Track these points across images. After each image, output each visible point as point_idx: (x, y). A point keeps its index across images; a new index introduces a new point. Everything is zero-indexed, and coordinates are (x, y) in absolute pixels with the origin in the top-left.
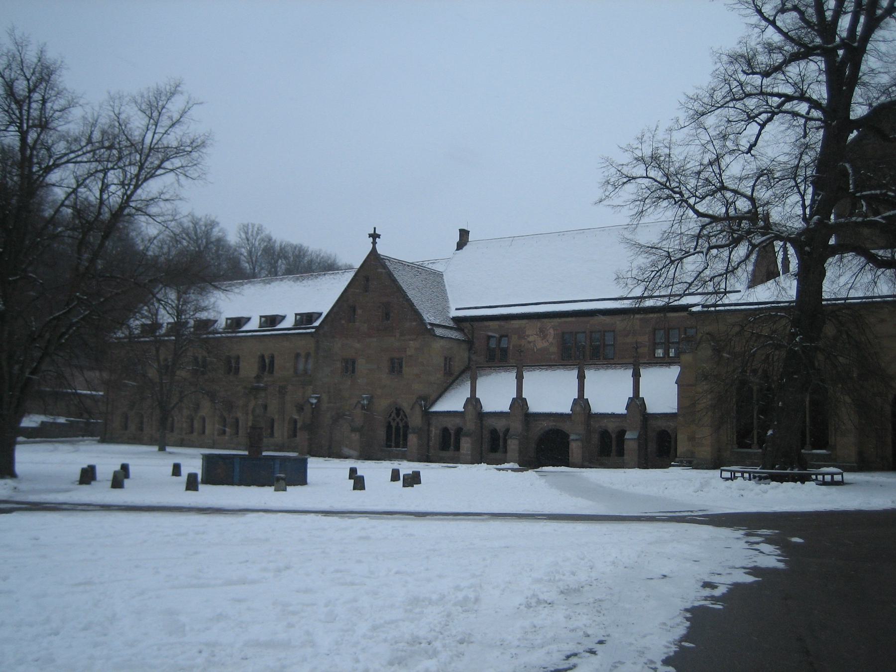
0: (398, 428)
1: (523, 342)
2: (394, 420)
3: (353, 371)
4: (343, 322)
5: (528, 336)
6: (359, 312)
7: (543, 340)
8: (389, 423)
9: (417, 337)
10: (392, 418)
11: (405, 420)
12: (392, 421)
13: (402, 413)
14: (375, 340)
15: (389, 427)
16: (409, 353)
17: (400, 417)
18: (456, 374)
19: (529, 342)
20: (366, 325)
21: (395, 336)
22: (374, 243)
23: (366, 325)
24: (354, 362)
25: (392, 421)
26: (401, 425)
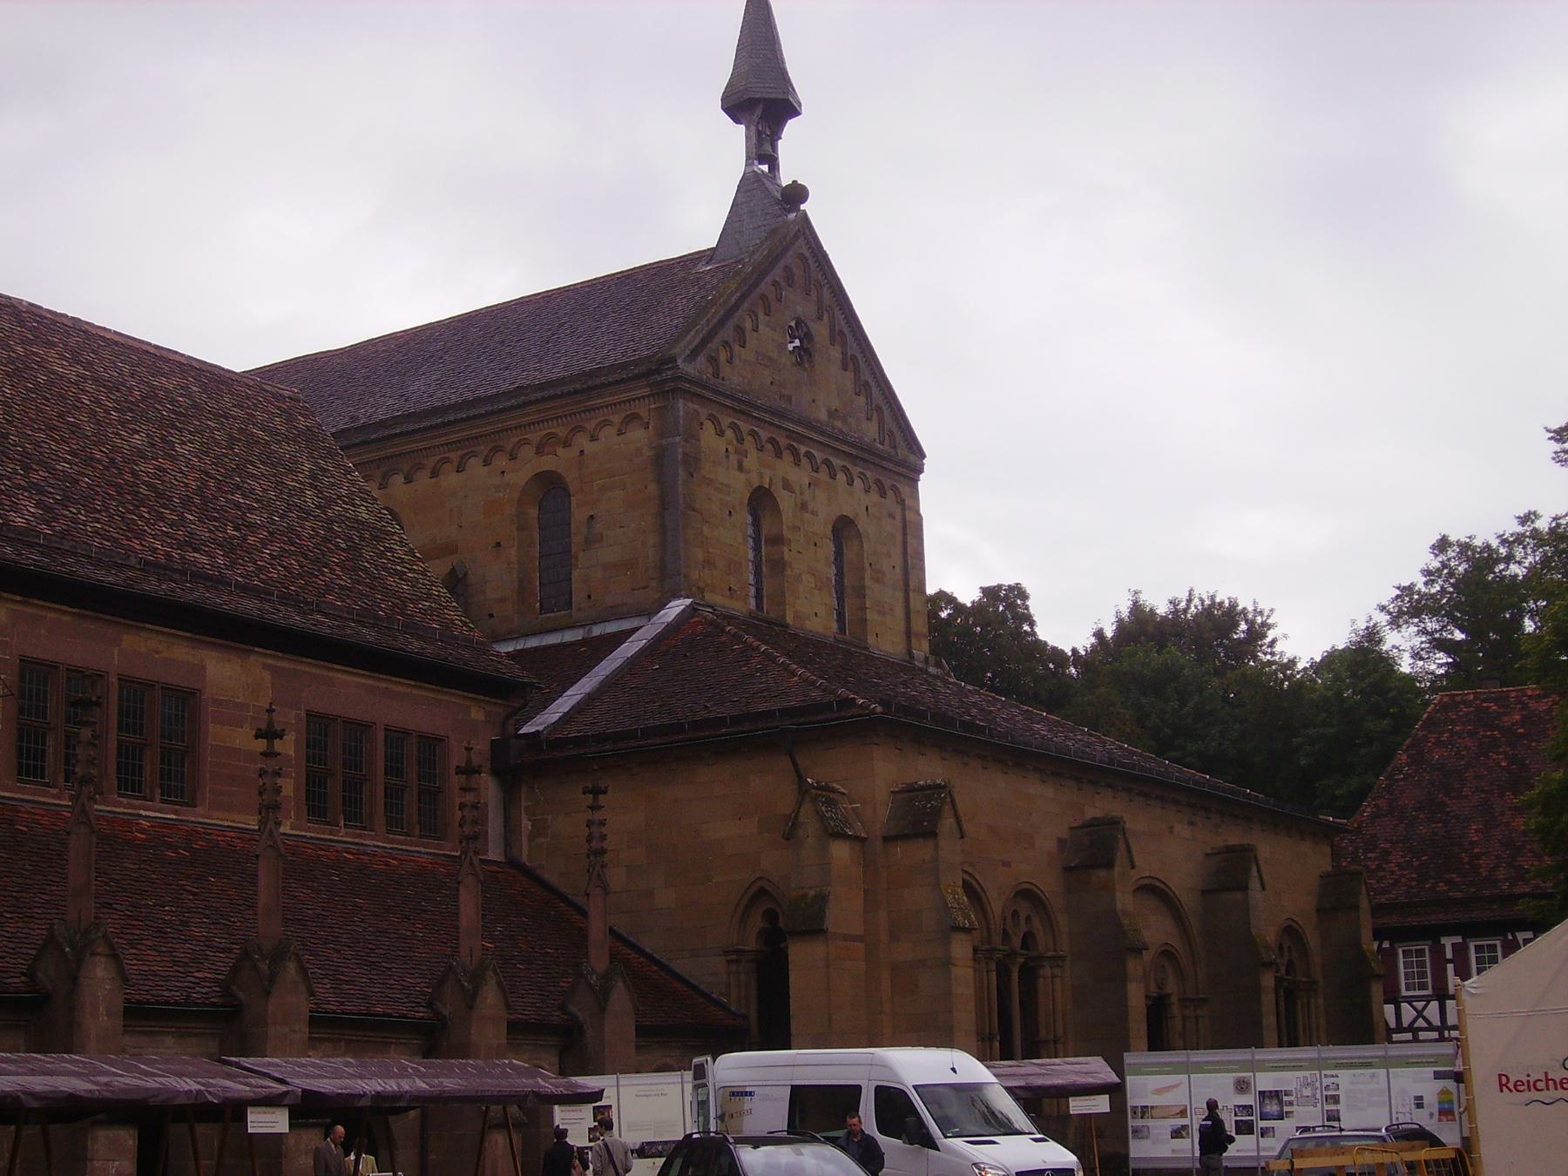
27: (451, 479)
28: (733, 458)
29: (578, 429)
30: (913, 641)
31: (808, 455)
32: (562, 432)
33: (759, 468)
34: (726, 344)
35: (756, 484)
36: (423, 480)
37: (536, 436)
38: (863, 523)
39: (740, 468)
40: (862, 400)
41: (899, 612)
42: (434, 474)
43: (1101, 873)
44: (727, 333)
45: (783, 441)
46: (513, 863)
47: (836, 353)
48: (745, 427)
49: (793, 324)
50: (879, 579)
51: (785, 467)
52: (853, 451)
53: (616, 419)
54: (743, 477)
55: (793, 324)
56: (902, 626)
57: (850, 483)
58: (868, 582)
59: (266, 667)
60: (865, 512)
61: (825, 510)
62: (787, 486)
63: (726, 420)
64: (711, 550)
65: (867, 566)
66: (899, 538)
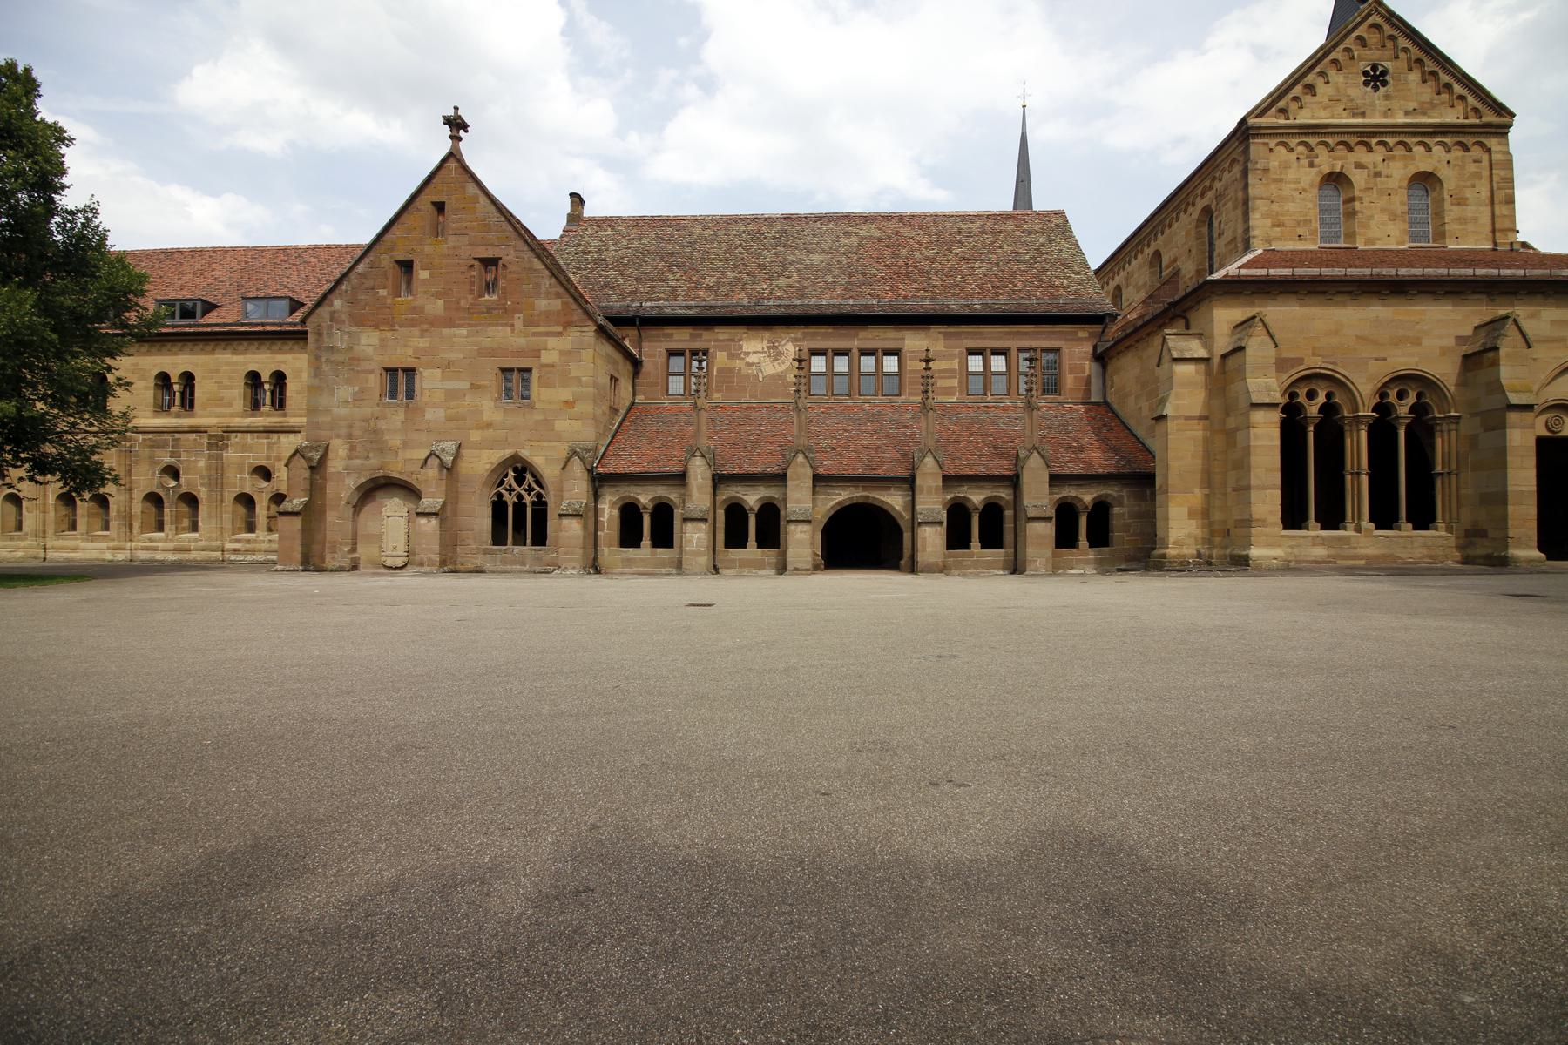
0: (520, 507)
1: (738, 363)
2: (510, 490)
3: (410, 394)
4: (383, 292)
5: (748, 354)
6: (422, 274)
7: (774, 360)
8: (500, 495)
9: (565, 328)
10: (506, 485)
11: (538, 489)
12: (503, 492)
13: (528, 476)
14: (464, 331)
15: (499, 507)
16: (546, 358)
17: (525, 485)
18: (623, 412)
19: (750, 365)
20: (440, 302)
21: (512, 326)
22: (456, 138)
23: (440, 302)
24: (410, 372)
25: (503, 492)
26: (528, 499)
27: (1175, 225)
28: (1305, 162)
29: (1214, 179)
30: (1497, 234)
31: (1380, 143)
32: (1208, 183)
33: (1326, 162)
34: (1296, 99)
35: (1327, 170)
36: (1167, 231)
37: (1199, 192)
38: (1444, 173)
39: (1311, 165)
40: (1445, 96)
41: (1485, 218)
42: (1170, 226)
43: (1491, 355)
44: (1297, 91)
45: (1352, 141)
46: (1106, 403)
47: (1414, 76)
48: (1312, 141)
49: (1369, 68)
50: (1461, 202)
51: (1361, 154)
52: (1431, 130)
53: (1226, 165)
54: (1314, 170)
55: (1369, 68)
56: (1488, 228)
57: (1429, 150)
58: (1447, 205)
59: (940, 333)
60: (1446, 166)
61: (1398, 171)
62: (1359, 166)
63: (1293, 142)
64: (1280, 217)
65: (1446, 197)
66: (1486, 173)
